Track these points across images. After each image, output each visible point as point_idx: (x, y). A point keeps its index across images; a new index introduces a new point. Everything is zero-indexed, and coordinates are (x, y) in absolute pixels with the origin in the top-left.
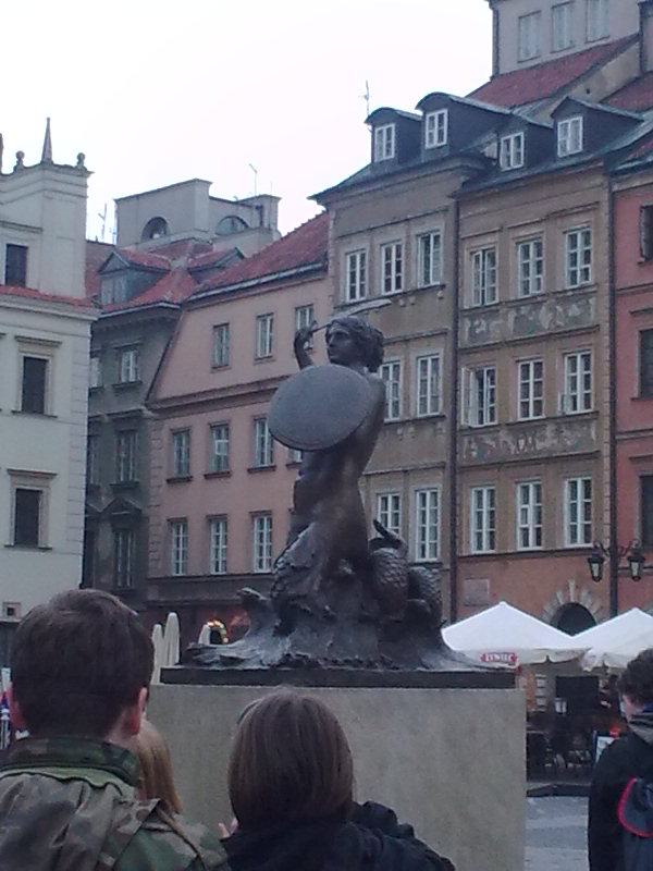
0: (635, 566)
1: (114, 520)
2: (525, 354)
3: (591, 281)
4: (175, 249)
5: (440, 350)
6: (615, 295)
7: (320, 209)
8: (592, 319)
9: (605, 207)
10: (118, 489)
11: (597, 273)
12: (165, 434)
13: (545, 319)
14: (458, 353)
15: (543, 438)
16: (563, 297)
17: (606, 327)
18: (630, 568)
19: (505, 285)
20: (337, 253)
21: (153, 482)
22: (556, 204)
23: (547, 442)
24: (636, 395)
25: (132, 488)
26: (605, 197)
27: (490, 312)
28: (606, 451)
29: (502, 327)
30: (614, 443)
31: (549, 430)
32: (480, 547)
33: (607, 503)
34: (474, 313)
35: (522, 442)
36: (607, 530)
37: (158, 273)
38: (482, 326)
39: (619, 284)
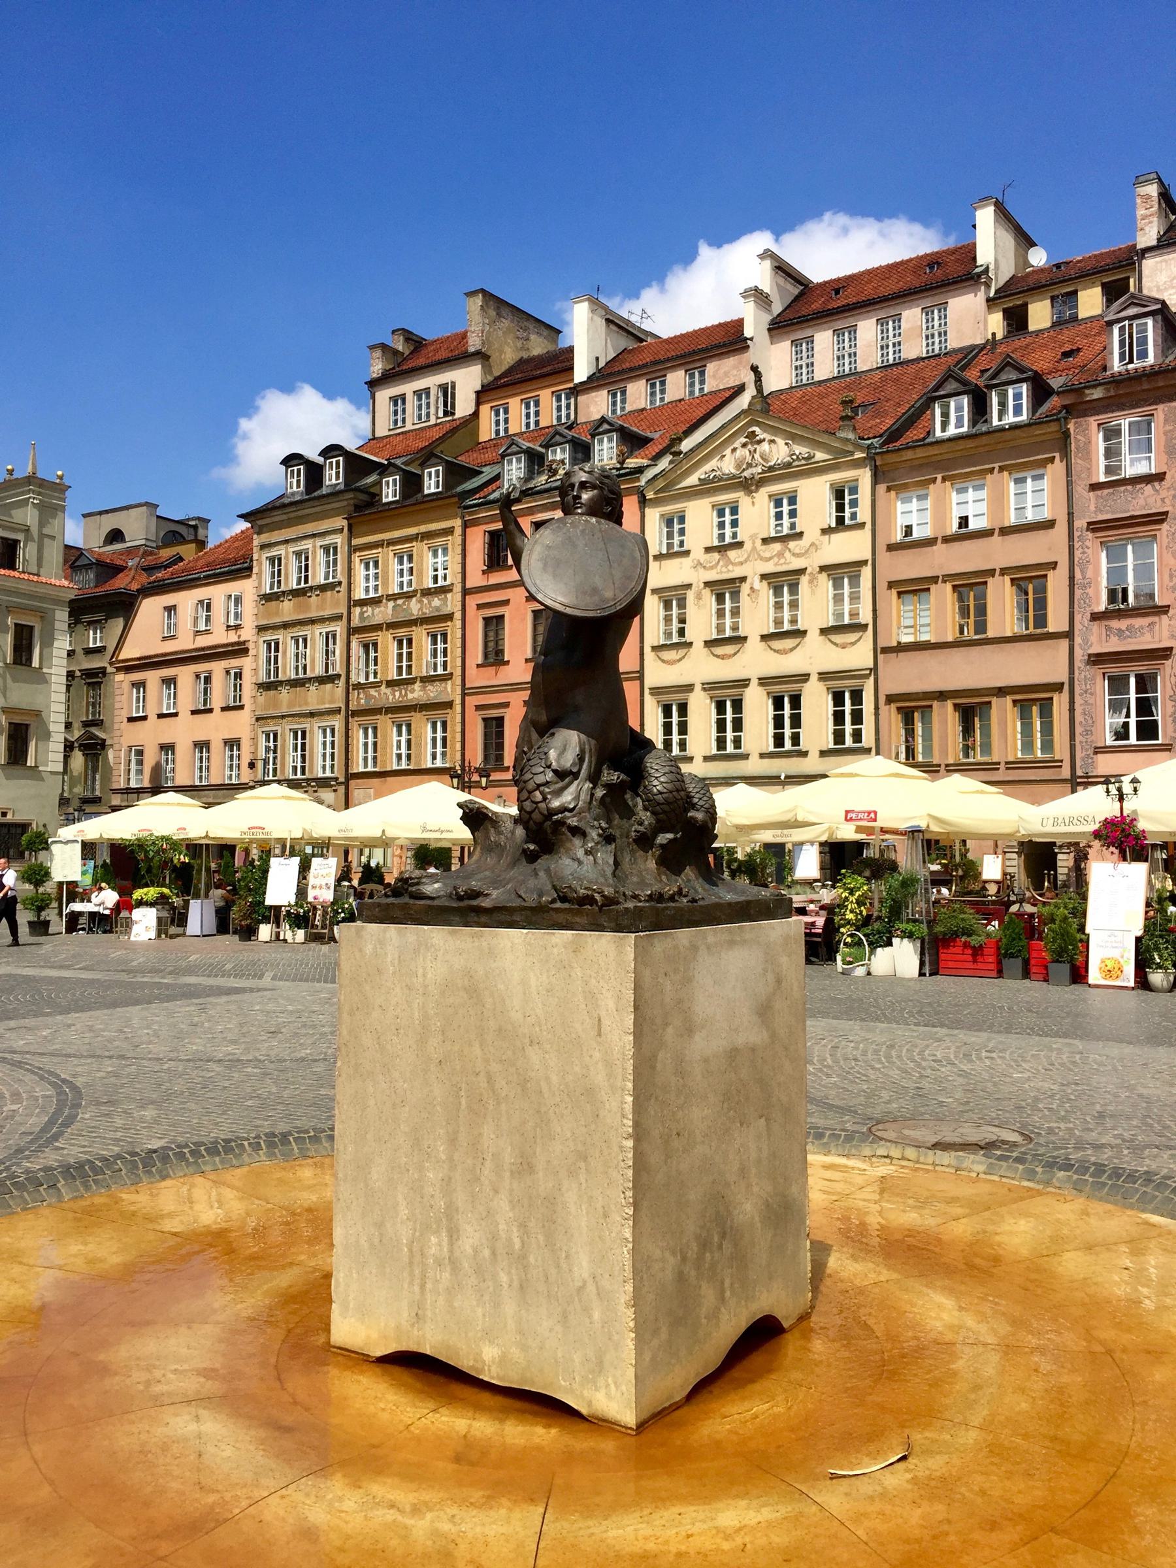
0: (484, 780)
1: (84, 748)
2: (401, 632)
3: (448, 582)
4: (131, 551)
5: (339, 628)
6: (466, 592)
7: (244, 525)
8: (447, 610)
9: (458, 531)
10: (86, 724)
11: (453, 578)
12: (126, 686)
13: (415, 608)
14: (352, 631)
15: (413, 691)
16: (427, 593)
17: (458, 615)
18: (480, 782)
19: (386, 583)
20: (260, 556)
21: (117, 719)
22: (423, 528)
23: (416, 694)
24: (480, 662)
25: (98, 723)
26: (457, 523)
27: (376, 602)
28: (458, 700)
29: (384, 613)
30: (464, 695)
31: (417, 686)
32: (366, 766)
33: (458, 737)
34: (362, 603)
35: (397, 694)
36: (458, 756)
37: (120, 569)
38: (369, 610)
39: (468, 586)
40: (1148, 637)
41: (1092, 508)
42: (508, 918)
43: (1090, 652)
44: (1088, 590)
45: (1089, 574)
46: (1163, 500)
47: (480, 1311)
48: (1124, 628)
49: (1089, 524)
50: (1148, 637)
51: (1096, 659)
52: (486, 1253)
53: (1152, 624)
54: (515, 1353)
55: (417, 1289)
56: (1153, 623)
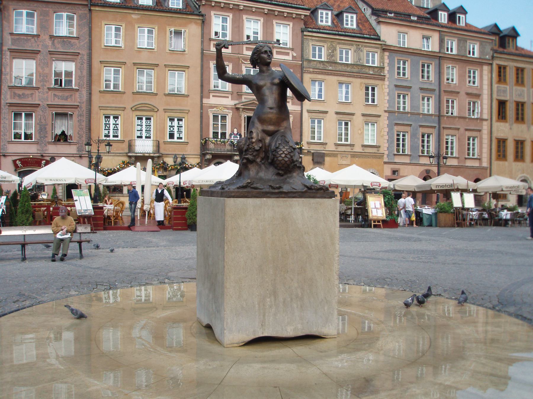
40: (30, 99)
41: (10, 42)
42: (294, 195)
43: (8, 102)
44: (7, 77)
45: (8, 70)
46: (38, 45)
47: (286, 317)
48: (21, 94)
49: (9, 49)
50: (30, 99)
51: (11, 105)
52: (289, 299)
53: (32, 94)
54: (299, 326)
55: (262, 317)
56: (32, 94)
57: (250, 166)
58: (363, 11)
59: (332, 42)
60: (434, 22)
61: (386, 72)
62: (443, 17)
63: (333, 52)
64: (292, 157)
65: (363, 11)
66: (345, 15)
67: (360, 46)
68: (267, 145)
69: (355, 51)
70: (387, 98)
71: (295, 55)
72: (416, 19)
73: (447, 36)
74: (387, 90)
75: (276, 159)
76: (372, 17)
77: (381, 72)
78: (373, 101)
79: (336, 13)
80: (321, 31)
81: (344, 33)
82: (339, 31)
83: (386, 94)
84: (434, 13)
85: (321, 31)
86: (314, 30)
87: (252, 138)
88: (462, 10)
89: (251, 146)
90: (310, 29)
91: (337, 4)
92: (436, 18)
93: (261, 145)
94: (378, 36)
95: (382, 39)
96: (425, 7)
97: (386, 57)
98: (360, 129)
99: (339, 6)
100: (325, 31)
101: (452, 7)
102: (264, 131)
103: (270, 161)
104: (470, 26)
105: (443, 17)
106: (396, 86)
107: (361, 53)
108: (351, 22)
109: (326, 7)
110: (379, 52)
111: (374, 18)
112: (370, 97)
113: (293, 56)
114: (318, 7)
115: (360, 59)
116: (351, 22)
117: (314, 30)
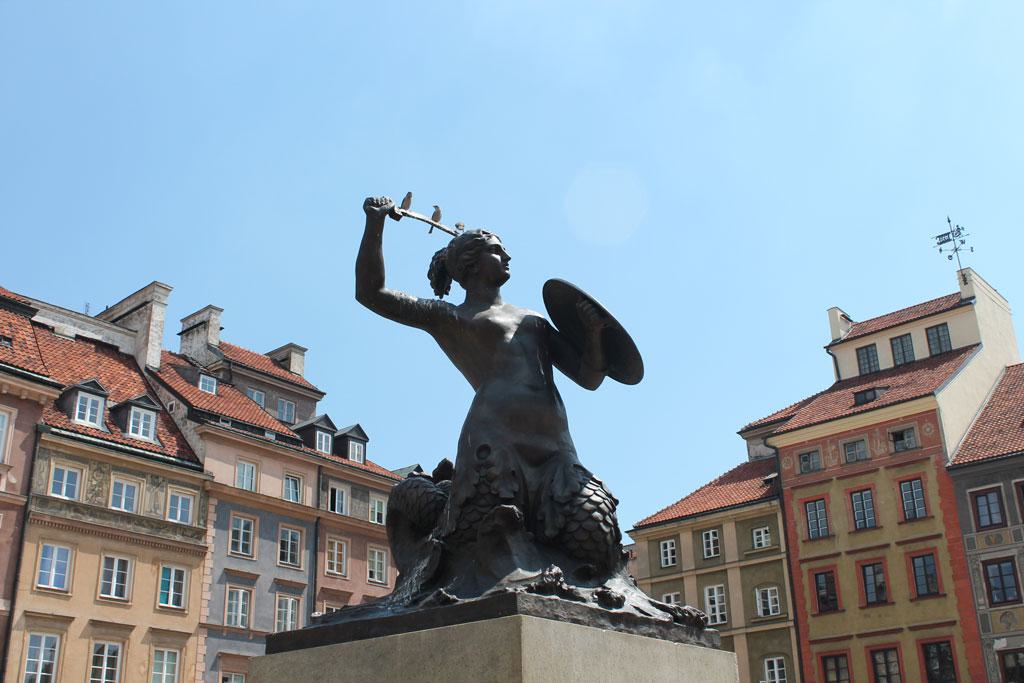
57: (510, 540)
58: (168, 408)
59: (100, 463)
60: (309, 450)
61: (209, 540)
62: (324, 444)
63: (100, 484)
64: (615, 521)
65: (168, 408)
66: (134, 409)
67: (161, 480)
68: (533, 487)
69: (148, 489)
70: (207, 596)
71: (13, 480)
72: (272, 437)
73: (332, 478)
74: (208, 580)
75: (574, 527)
76: (189, 422)
77: (200, 539)
78: (177, 601)
79: (111, 404)
80: (80, 436)
81: (128, 448)
82: (117, 443)
83: (206, 587)
84: (307, 435)
85: (80, 436)
86: (63, 432)
87: (489, 465)
88: (360, 435)
89: (484, 489)
90: (54, 430)
91: (114, 388)
92: (311, 444)
93: (516, 487)
94: (198, 462)
95: (206, 468)
96: (285, 419)
97: (212, 509)
98: (144, 664)
99: (118, 392)
100: (88, 438)
101: (342, 425)
102: (520, 449)
103: (549, 532)
104: (372, 465)
105: (324, 444)
106: (227, 571)
107: (162, 495)
108: (143, 429)
109: (95, 388)
110: (198, 499)
111: (191, 424)
112: (172, 592)
113: (9, 485)
114: (79, 383)
115: (156, 508)
116: (143, 429)
117: (63, 432)
